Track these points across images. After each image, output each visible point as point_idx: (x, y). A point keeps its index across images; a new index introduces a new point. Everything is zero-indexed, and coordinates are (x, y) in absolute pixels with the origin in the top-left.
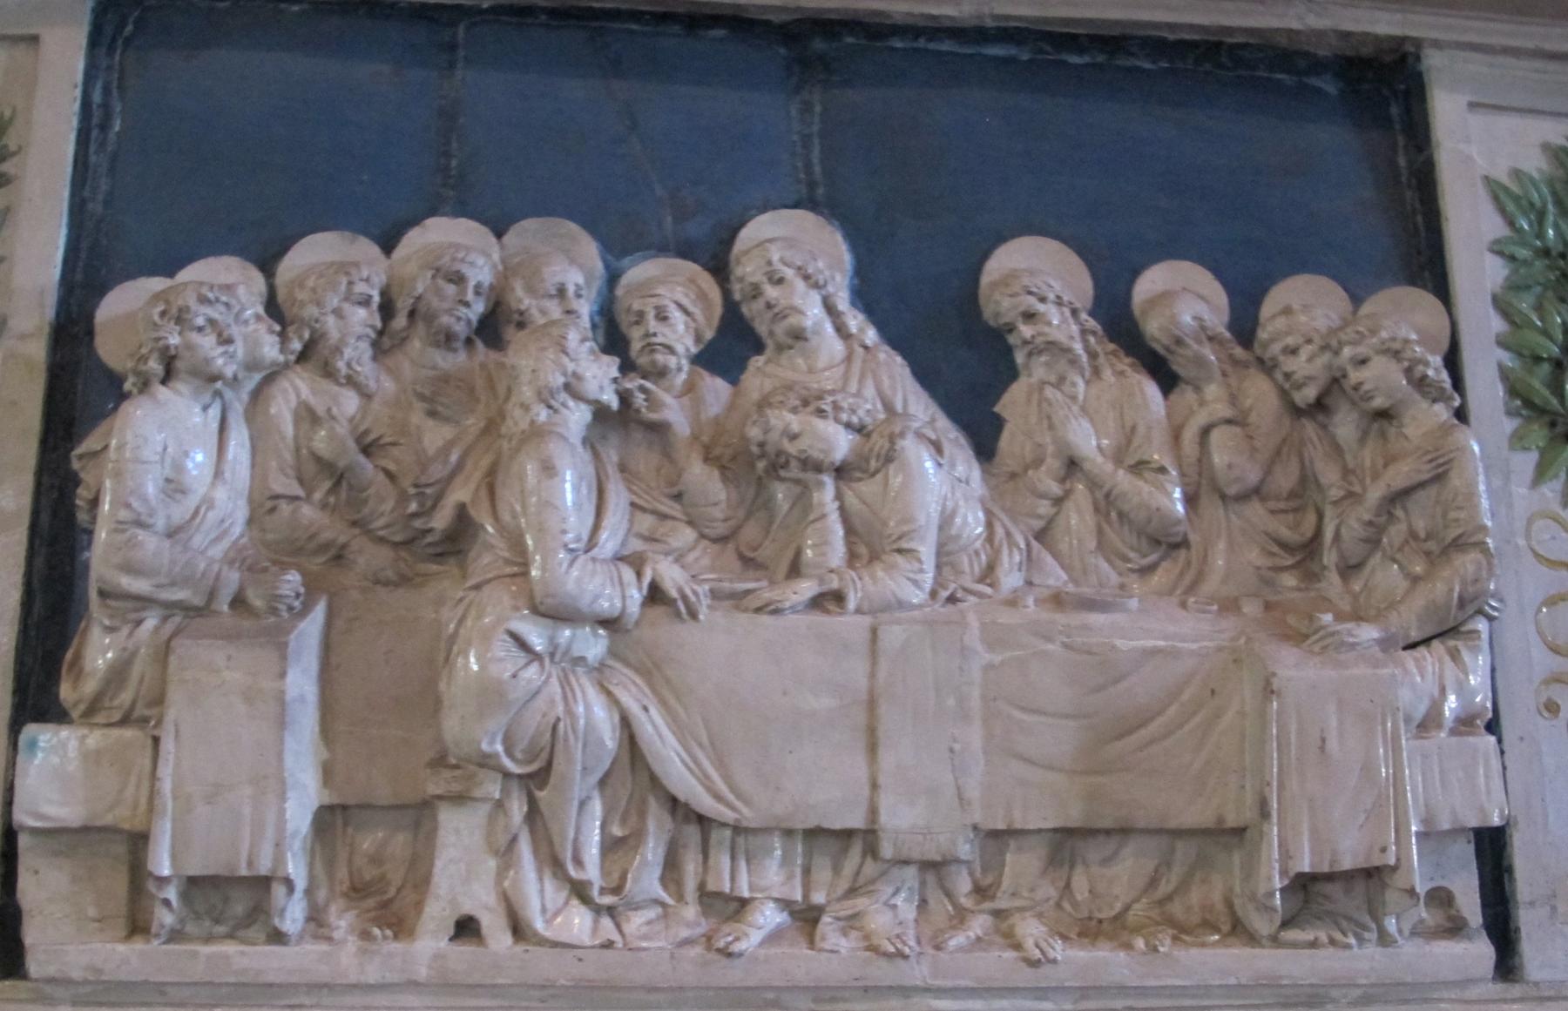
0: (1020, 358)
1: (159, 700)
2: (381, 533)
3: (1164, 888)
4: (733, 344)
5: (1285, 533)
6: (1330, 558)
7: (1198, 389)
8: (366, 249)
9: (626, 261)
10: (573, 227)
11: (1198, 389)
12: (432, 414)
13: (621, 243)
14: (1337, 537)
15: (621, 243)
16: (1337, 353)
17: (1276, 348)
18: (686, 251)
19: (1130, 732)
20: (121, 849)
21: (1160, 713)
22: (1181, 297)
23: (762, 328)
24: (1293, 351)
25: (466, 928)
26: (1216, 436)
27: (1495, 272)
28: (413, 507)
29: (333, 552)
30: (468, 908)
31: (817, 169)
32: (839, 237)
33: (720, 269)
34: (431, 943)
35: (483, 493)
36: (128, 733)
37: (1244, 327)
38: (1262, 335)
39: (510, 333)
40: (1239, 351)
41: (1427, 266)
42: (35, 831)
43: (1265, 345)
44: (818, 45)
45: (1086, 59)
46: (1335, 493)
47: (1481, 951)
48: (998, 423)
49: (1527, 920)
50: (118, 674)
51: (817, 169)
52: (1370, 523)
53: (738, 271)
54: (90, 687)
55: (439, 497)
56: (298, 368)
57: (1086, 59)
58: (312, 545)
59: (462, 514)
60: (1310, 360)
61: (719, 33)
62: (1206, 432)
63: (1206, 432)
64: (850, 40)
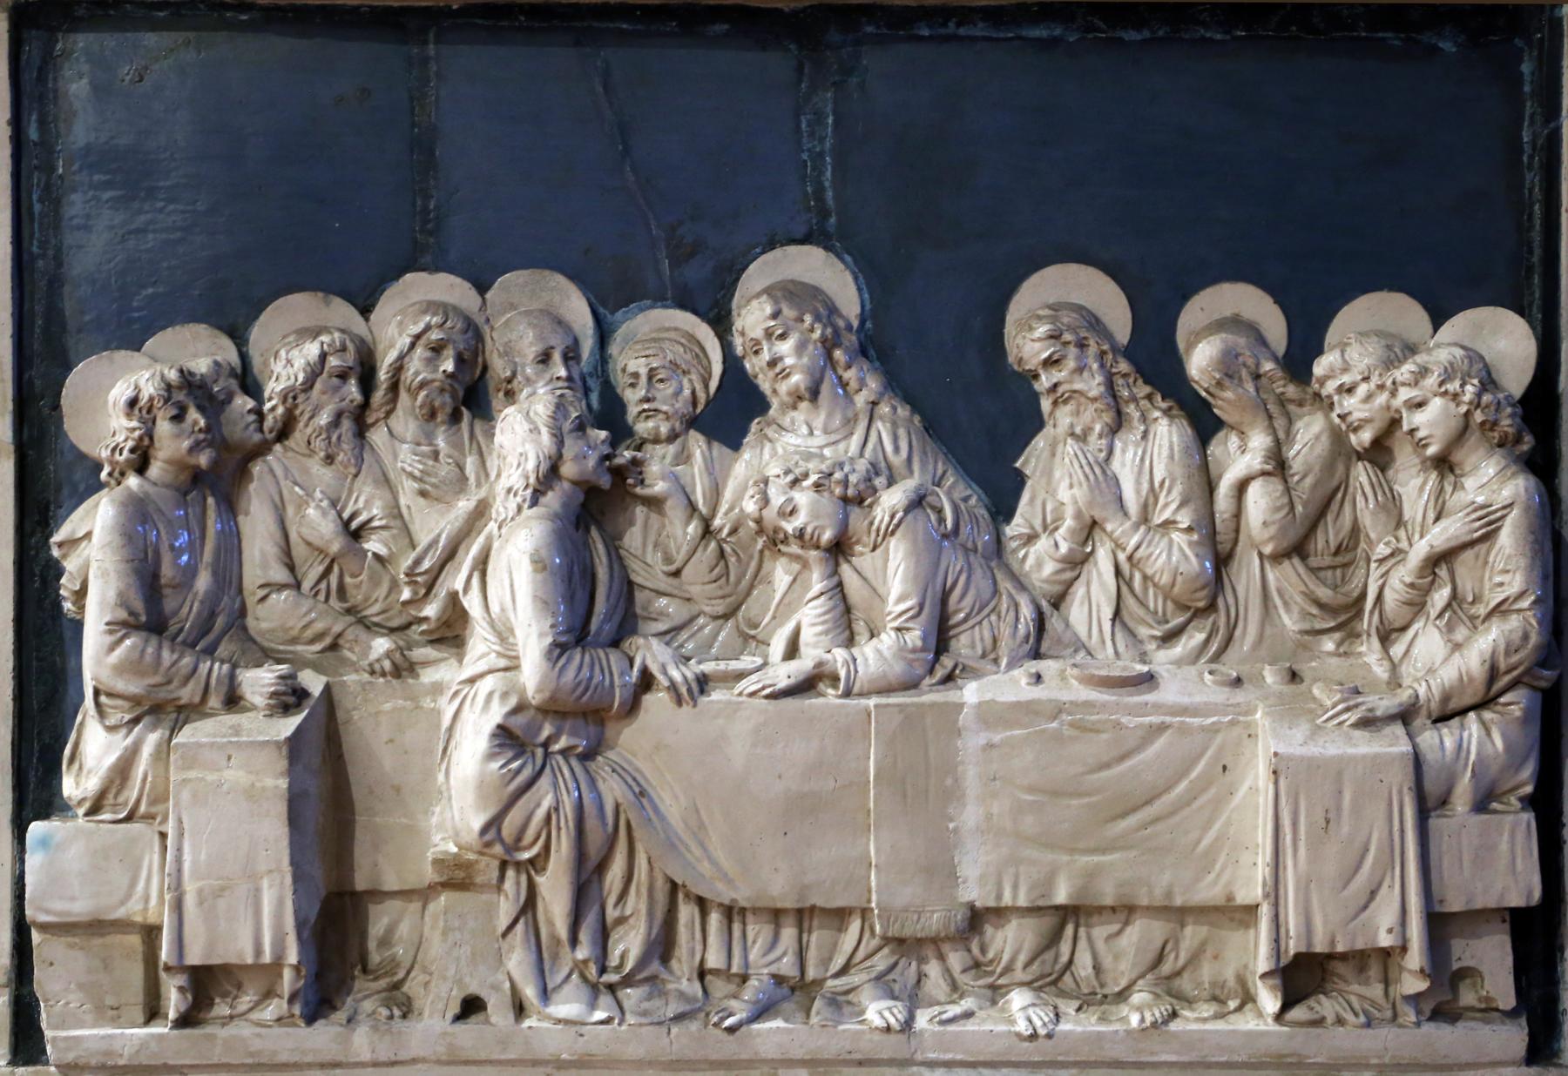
0: (1046, 404)
1: (160, 798)
2: (375, 619)
3: (1167, 968)
5: (1324, 593)
6: (1368, 621)
7: (1242, 434)
8: (342, 312)
9: (619, 314)
10: (560, 280)
11: (1242, 434)
12: (423, 494)
13: (613, 296)
14: (1379, 598)
15: (613, 296)
16: (1394, 394)
17: (1330, 387)
19: (1134, 810)
20: (135, 941)
21: (1167, 789)
23: (765, 385)
24: (1350, 390)
25: (471, 1007)
26: (1255, 492)
28: (406, 594)
29: (328, 641)
30: (474, 988)
31: (830, 194)
32: (849, 278)
33: (721, 322)
34: (432, 1025)
35: (475, 581)
36: (135, 827)
37: (1298, 363)
38: (1319, 368)
39: (497, 399)
40: (1291, 390)
42: (44, 927)
43: (1322, 382)
45: (1146, 34)
46: (1382, 550)
47: (1514, 1037)
48: (1018, 481)
50: (122, 771)
51: (830, 194)
52: (1412, 585)
53: (738, 324)
54: (92, 784)
55: (430, 587)
56: (278, 447)
57: (1146, 34)
58: (309, 633)
59: (454, 598)
60: (1369, 398)
61: (721, 28)
62: (1242, 487)
63: (1242, 487)
64: (870, 29)
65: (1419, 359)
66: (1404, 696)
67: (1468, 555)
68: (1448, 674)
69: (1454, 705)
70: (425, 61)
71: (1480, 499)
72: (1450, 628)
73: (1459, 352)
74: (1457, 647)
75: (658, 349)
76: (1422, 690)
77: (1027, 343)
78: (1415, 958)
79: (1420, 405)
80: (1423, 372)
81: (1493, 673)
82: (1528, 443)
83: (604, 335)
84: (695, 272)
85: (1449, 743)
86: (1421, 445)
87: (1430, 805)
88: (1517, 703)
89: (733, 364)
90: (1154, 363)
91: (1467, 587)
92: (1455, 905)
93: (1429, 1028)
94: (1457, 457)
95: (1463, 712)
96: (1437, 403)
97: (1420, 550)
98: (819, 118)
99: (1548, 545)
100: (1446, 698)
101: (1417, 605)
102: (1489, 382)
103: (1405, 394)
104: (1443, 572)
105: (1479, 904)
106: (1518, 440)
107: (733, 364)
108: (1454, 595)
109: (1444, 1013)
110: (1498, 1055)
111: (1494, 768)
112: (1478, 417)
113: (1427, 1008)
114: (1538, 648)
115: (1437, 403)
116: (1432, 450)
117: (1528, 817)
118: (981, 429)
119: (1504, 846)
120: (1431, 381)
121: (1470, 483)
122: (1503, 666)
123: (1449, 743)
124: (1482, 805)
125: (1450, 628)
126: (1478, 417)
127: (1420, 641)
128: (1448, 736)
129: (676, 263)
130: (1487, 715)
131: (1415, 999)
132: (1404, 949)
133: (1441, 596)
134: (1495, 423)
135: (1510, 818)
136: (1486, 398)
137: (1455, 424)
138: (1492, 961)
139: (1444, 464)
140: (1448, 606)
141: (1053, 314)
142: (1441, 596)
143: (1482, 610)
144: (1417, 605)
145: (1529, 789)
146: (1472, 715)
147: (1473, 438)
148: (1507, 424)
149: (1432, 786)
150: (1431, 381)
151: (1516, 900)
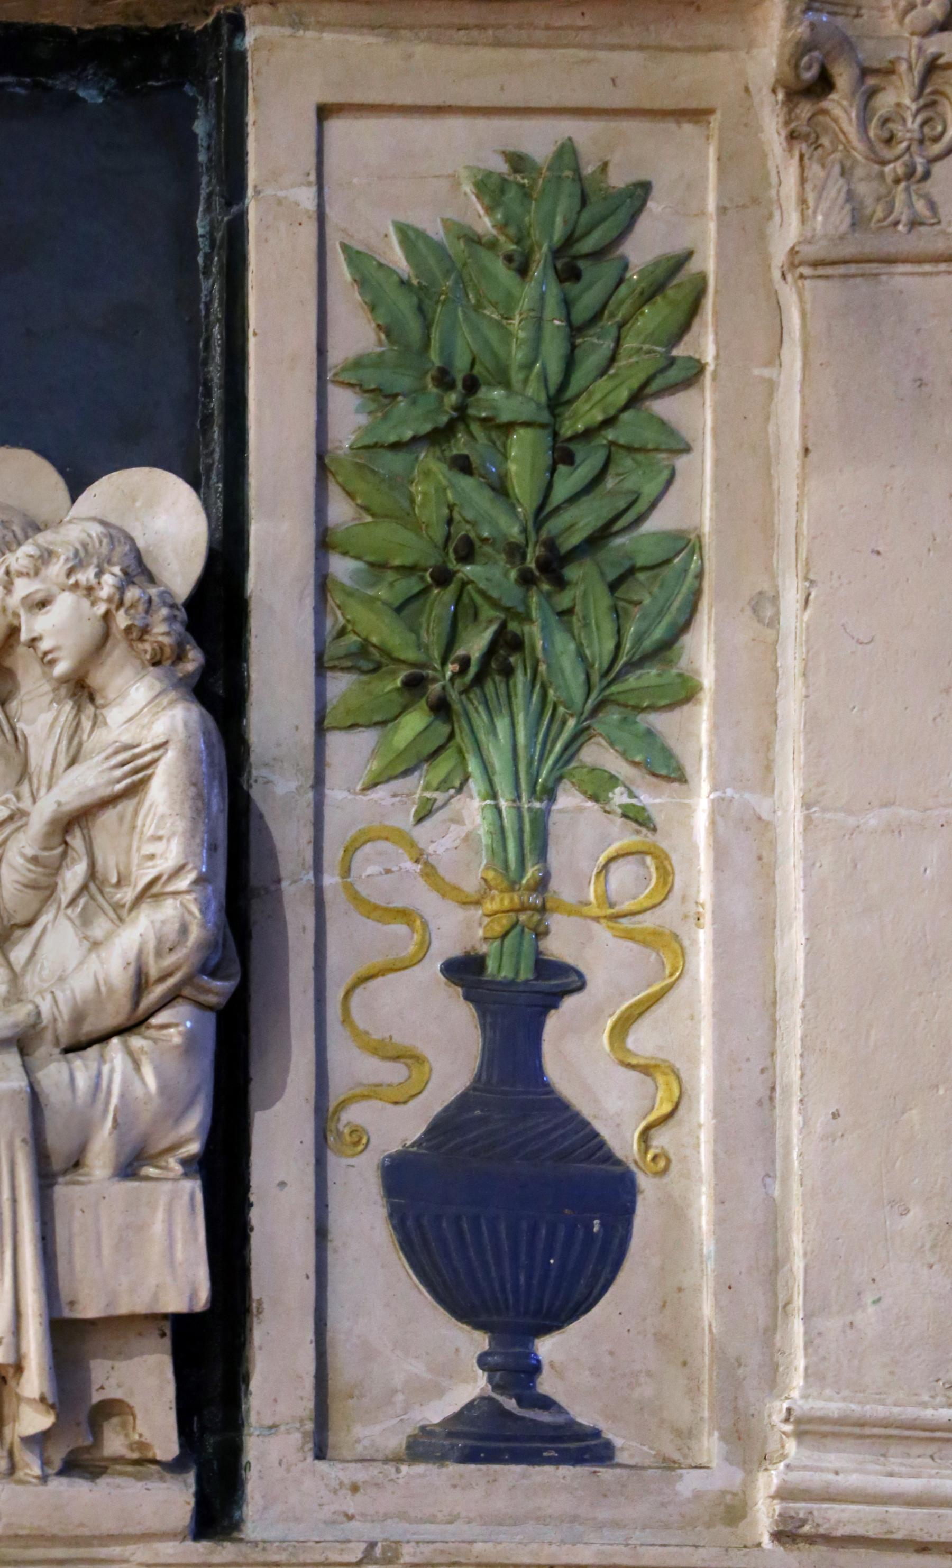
65: (41, 538)
66: (21, 1013)
67: (109, 816)
68: (81, 984)
69: (90, 1027)
71: (126, 738)
72: (86, 920)
73: (96, 530)
74: (96, 945)
76: (46, 1007)
78: (34, 1381)
79: (43, 604)
80: (46, 556)
81: (141, 984)
82: (194, 660)
85: (83, 1081)
86: (47, 661)
87: (57, 1164)
88: (177, 1025)
91: (109, 865)
92: (90, 1307)
93: (59, 1485)
94: (96, 679)
95: (104, 1038)
96: (65, 603)
97: (43, 811)
99: (218, 804)
100: (78, 1018)
101: (44, 889)
102: (139, 570)
103: (22, 587)
104: (76, 841)
105: (123, 1309)
106: (180, 657)
108: (92, 872)
109: (81, 1465)
110: (153, 1524)
111: (146, 1117)
112: (122, 620)
113: (58, 1456)
114: (202, 946)
115: (65, 603)
116: (61, 668)
117: (193, 1187)
119: (158, 1227)
120: (56, 569)
121: (115, 716)
122: (153, 971)
123: (83, 1081)
124: (131, 1166)
125: (86, 920)
126: (122, 620)
127: (49, 942)
128: (82, 1069)
130: (136, 1042)
131: (39, 1441)
132: (19, 1368)
133: (73, 876)
134: (145, 631)
135: (167, 1186)
136: (132, 593)
137: (90, 629)
138: (145, 1387)
139: (81, 689)
140: (84, 888)
142: (73, 876)
143: (127, 895)
144: (44, 889)
145: (194, 1148)
146: (115, 1041)
147: (118, 651)
148: (162, 631)
149: (59, 1142)
150: (56, 569)
151: (175, 1304)
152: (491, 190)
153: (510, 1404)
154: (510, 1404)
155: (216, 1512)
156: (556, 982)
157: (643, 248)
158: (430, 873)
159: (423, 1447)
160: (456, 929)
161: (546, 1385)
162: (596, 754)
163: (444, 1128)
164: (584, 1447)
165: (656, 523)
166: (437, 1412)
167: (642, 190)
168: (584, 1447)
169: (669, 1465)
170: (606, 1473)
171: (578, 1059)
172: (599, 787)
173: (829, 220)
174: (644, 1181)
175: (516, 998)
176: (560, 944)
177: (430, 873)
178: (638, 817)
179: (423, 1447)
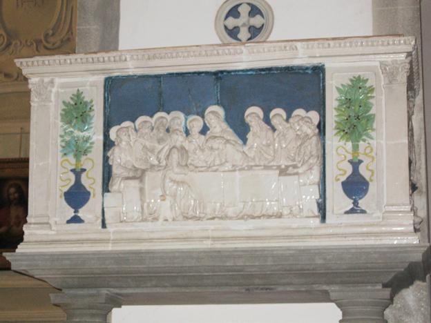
4: (204, 131)
18: (198, 114)
22: (278, 113)
27: (336, 104)
33: (203, 117)
41: (321, 107)
44: (220, 75)
49: (328, 214)
70: (160, 82)
75: (196, 123)
77: (248, 120)
83: (186, 119)
84: (199, 110)
89: (205, 124)
90: (267, 120)
98: (217, 87)
107: (205, 124)
118: (241, 130)
129: (197, 109)
141: (253, 114)
152: (351, 80)
153: (355, 208)
154: (355, 208)
155: (323, 218)
156: (360, 162)
157: (368, 85)
158: (346, 151)
159: (347, 213)
160: (350, 157)
161: (359, 205)
162: (364, 137)
163: (348, 178)
164: (363, 212)
165: (371, 113)
166: (348, 209)
167: (367, 80)
168: (363, 212)
169: (373, 214)
170: (366, 215)
171: (362, 170)
172: (364, 141)
173: (387, 82)
174: (370, 183)
175: (355, 164)
176: (360, 157)
177: (346, 151)
178: (369, 143)
179: (347, 213)
